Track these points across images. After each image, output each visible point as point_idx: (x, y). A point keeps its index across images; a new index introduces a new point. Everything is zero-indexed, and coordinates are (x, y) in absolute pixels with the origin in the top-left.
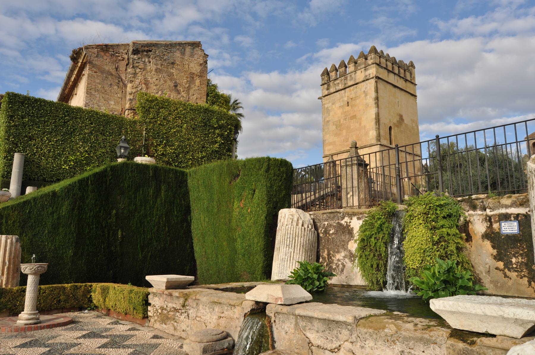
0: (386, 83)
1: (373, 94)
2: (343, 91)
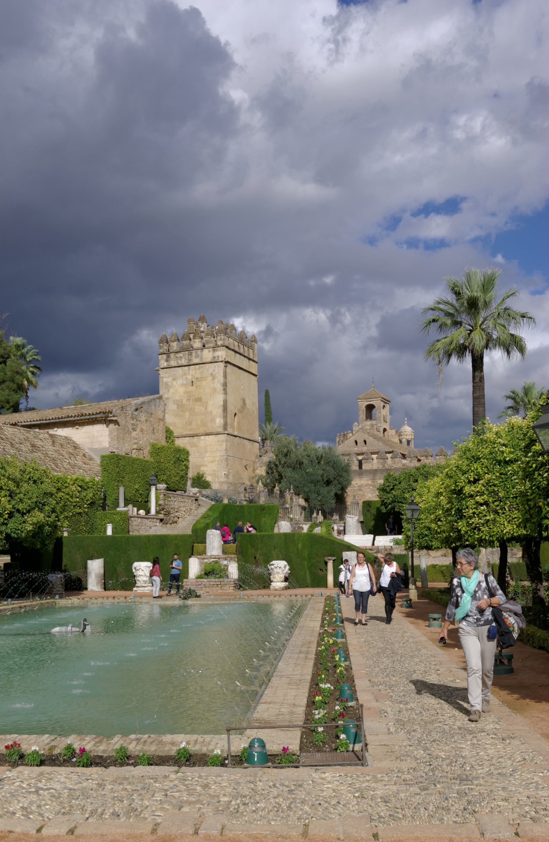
1: (222, 379)
2: (186, 368)
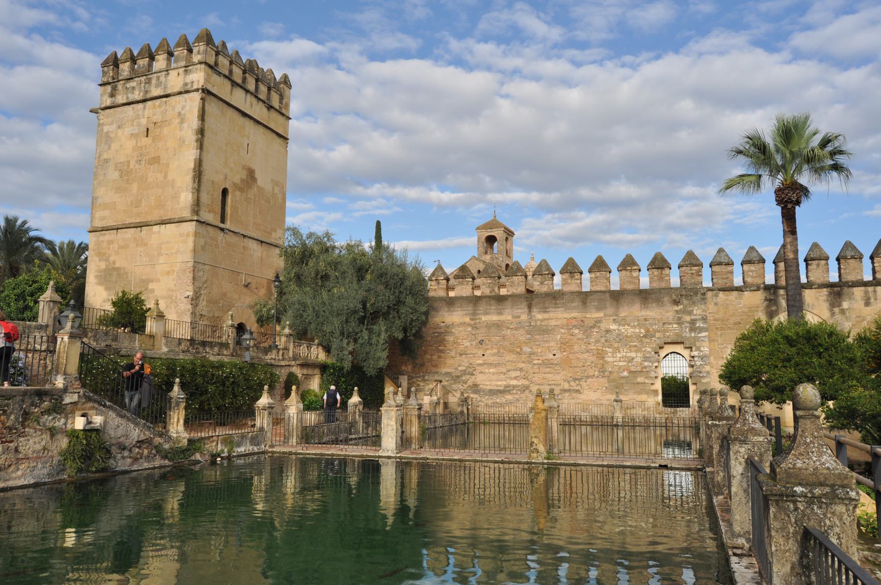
0: (225, 105)
1: (195, 123)
2: (141, 105)
